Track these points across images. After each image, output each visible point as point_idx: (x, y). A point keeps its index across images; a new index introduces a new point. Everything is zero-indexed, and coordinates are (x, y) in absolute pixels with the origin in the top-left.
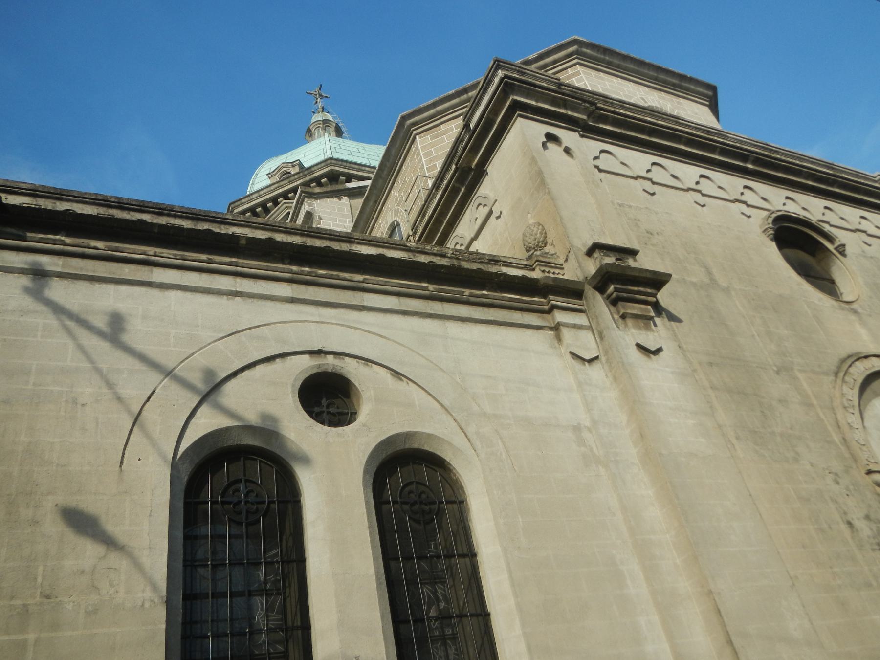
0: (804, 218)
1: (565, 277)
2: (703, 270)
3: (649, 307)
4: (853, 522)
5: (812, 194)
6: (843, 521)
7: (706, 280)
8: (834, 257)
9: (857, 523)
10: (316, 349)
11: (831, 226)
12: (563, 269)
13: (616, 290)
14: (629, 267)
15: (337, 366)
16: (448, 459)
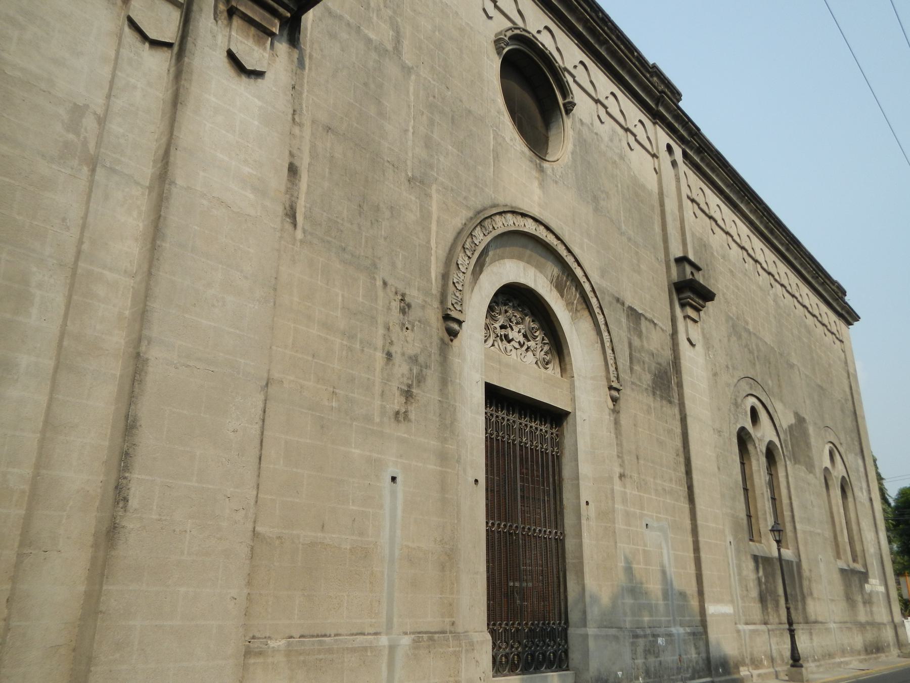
4: (394, 355)
5: (576, 42)
7: (390, 47)
8: (559, 113)
9: (397, 358)
11: (575, 81)
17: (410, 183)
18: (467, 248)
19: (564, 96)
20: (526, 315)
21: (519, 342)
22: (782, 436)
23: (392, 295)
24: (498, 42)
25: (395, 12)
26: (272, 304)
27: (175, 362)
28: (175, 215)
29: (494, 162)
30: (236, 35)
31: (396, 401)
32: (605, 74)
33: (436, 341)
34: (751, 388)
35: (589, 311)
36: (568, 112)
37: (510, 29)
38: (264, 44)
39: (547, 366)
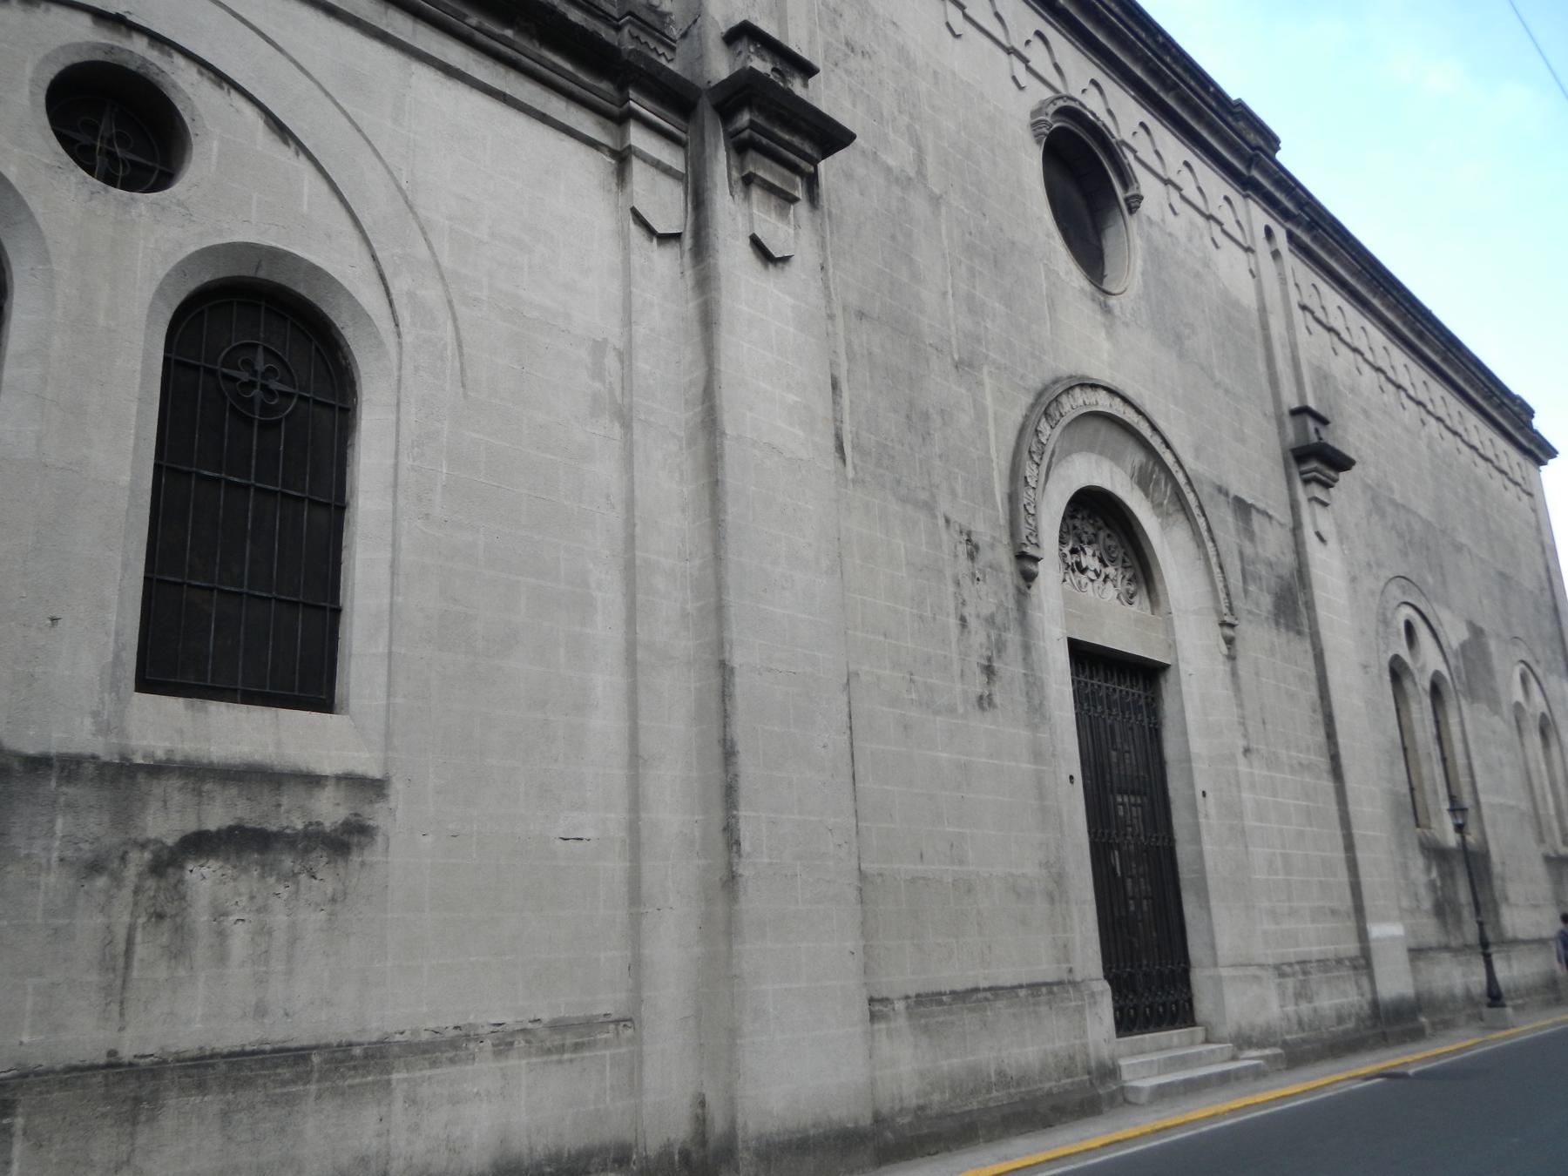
0: (1103, 128)
1: (671, 66)
2: (912, 150)
3: (798, 180)
4: (968, 618)
5: (1133, 93)
6: (956, 613)
7: (912, 174)
8: (1119, 213)
9: (973, 622)
10: (112, 11)
12: (673, 49)
13: (752, 125)
14: (790, 93)
15: (152, 64)
16: (339, 325)
17: (958, 370)
18: (1034, 452)
19: (1126, 186)
20: (1099, 529)
21: (1095, 571)
22: (1452, 661)
23: (956, 536)
24: (1035, 125)
25: (911, 116)
26: (839, 575)
27: (758, 667)
28: (732, 478)
29: (1050, 313)
30: (757, 213)
31: (977, 681)
32: (1175, 135)
33: (1011, 591)
34: (1404, 593)
35: (1186, 514)
36: (1132, 210)
37: (1053, 101)
38: (788, 213)
39: (1132, 600)
